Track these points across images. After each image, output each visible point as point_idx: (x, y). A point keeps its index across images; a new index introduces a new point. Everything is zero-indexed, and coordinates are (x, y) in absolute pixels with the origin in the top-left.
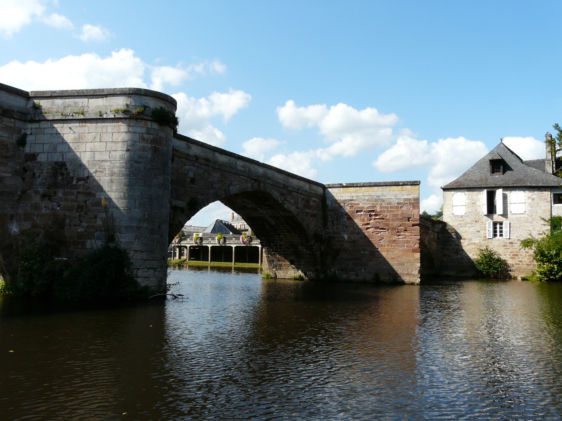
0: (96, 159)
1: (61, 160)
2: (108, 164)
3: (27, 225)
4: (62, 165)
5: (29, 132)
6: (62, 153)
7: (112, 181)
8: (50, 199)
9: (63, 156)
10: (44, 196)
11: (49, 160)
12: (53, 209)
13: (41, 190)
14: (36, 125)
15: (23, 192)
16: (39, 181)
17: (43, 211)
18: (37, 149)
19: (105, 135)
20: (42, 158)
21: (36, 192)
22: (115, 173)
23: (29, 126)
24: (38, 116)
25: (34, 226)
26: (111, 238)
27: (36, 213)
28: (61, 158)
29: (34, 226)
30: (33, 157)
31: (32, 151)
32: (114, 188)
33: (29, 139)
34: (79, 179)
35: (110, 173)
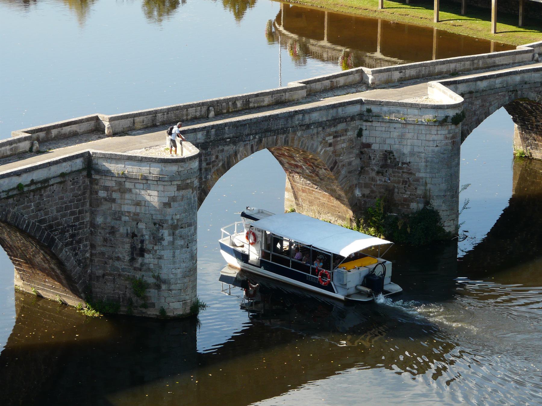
0: (415, 150)
1: (389, 149)
2: (423, 155)
3: (367, 191)
4: (391, 152)
5: (364, 128)
6: (390, 145)
7: (426, 166)
8: (382, 175)
9: (391, 147)
10: (378, 173)
11: (381, 148)
12: (385, 181)
13: (376, 168)
14: (369, 124)
15: (362, 168)
16: (373, 162)
17: (378, 182)
18: (371, 140)
19: (421, 135)
20: (375, 147)
21: (372, 170)
22: (428, 161)
23: (364, 123)
24: (371, 118)
25: (372, 191)
26: (427, 203)
27: (373, 183)
28: (389, 148)
29: (372, 191)
30: (369, 146)
31: (368, 142)
32: (428, 171)
33: (365, 133)
34: (403, 163)
35: (425, 161)
